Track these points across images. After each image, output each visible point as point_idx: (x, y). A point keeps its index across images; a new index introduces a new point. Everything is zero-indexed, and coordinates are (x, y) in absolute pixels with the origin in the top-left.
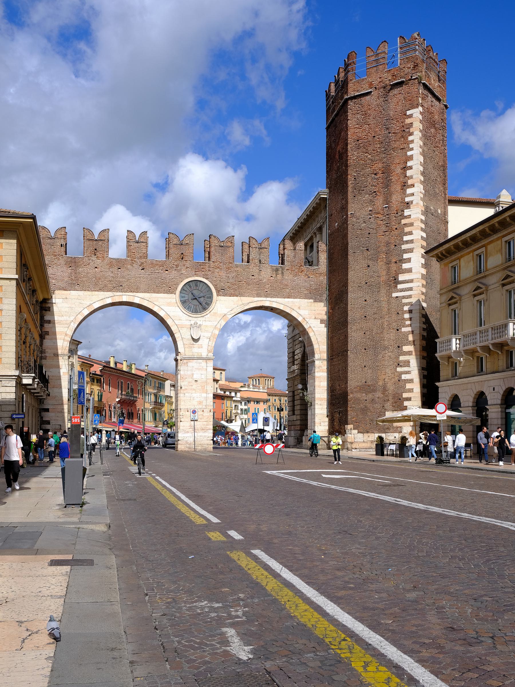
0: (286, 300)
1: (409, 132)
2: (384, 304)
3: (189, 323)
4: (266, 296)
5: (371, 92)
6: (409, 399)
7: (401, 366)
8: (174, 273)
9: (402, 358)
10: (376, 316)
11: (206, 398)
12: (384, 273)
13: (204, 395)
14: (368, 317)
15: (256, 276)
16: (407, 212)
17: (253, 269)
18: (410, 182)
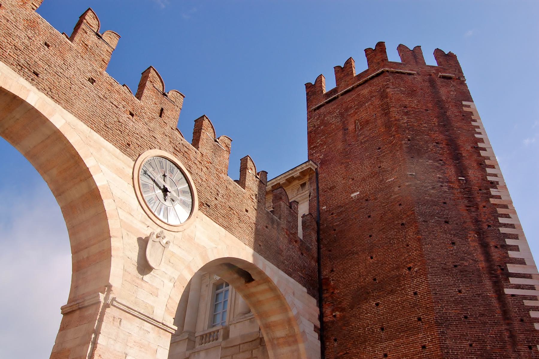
16: (493, 192)
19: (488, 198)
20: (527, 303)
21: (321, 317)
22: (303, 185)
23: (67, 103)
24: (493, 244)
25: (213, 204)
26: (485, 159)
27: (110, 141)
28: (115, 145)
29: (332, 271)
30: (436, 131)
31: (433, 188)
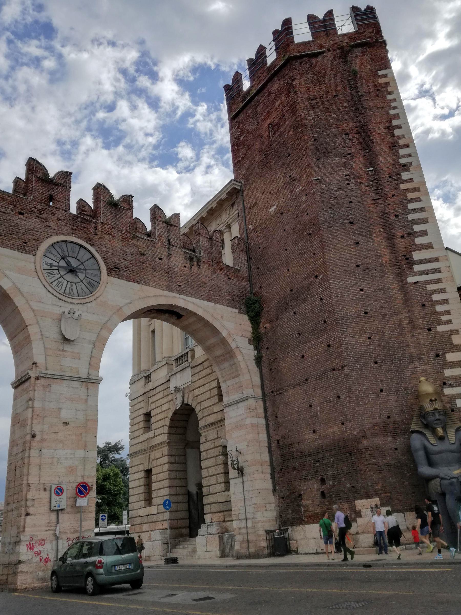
0: (206, 303)
1: (386, 91)
2: (397, 294)
3: (58, 311)
4: (180, 292)
5: (323, 53)
7: (451, 386)
8: (33, 222)
10: (384, 311)
11: (84, 460)
12: (387, 252)
13: (80, 453)
14: (371, 314)
15: (165, 261)
16: (405, 176)
17: (160, 249)
18: (401, 142)
19: (398, 184)
20: (430, 287)
22: (233, 205)
24: (400, 234)
25: (122, 265)
26: (399, 139)
27: (7, 247)
28: (12, 249)
29: (261, 287)
30: (346, 120)
31: (340, 189)
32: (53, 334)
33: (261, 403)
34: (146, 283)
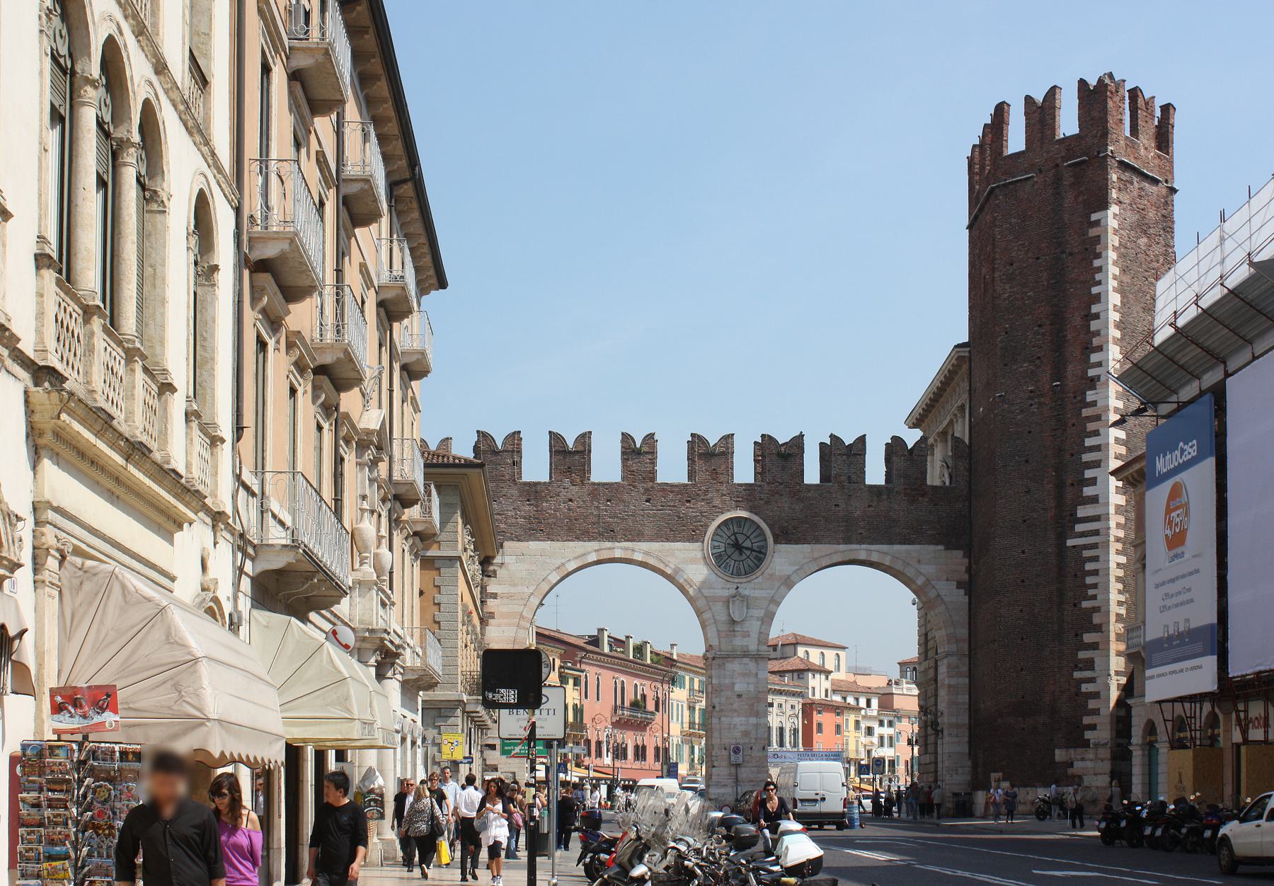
3: (726, 593)
4: (860, 542)
6: (1093, 727)
7: (1081, 669)
9: (1082, 655)
15: (843, 506)
20: (1086, 553)
21: (969, 570)
23: (637, 536)
32: (722, 617)
33: (966, 660)
34: (818, 541)
